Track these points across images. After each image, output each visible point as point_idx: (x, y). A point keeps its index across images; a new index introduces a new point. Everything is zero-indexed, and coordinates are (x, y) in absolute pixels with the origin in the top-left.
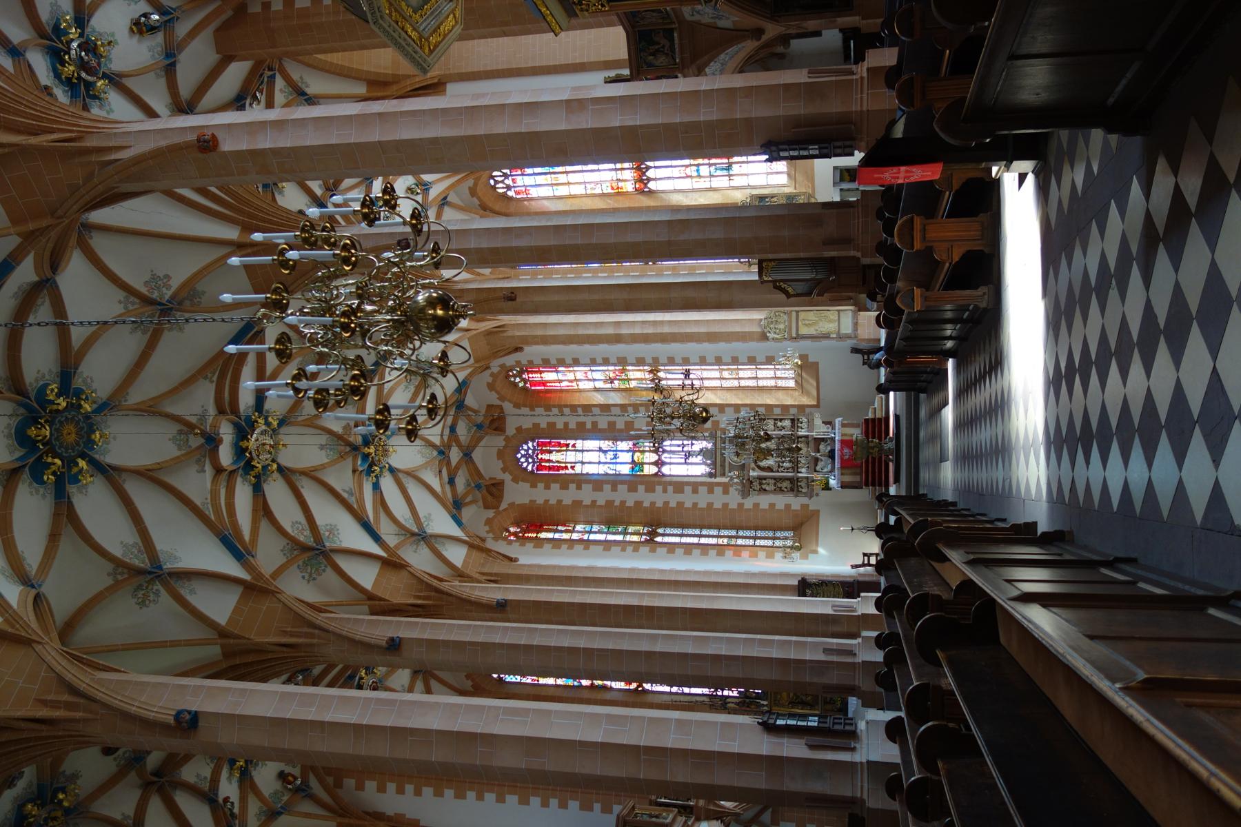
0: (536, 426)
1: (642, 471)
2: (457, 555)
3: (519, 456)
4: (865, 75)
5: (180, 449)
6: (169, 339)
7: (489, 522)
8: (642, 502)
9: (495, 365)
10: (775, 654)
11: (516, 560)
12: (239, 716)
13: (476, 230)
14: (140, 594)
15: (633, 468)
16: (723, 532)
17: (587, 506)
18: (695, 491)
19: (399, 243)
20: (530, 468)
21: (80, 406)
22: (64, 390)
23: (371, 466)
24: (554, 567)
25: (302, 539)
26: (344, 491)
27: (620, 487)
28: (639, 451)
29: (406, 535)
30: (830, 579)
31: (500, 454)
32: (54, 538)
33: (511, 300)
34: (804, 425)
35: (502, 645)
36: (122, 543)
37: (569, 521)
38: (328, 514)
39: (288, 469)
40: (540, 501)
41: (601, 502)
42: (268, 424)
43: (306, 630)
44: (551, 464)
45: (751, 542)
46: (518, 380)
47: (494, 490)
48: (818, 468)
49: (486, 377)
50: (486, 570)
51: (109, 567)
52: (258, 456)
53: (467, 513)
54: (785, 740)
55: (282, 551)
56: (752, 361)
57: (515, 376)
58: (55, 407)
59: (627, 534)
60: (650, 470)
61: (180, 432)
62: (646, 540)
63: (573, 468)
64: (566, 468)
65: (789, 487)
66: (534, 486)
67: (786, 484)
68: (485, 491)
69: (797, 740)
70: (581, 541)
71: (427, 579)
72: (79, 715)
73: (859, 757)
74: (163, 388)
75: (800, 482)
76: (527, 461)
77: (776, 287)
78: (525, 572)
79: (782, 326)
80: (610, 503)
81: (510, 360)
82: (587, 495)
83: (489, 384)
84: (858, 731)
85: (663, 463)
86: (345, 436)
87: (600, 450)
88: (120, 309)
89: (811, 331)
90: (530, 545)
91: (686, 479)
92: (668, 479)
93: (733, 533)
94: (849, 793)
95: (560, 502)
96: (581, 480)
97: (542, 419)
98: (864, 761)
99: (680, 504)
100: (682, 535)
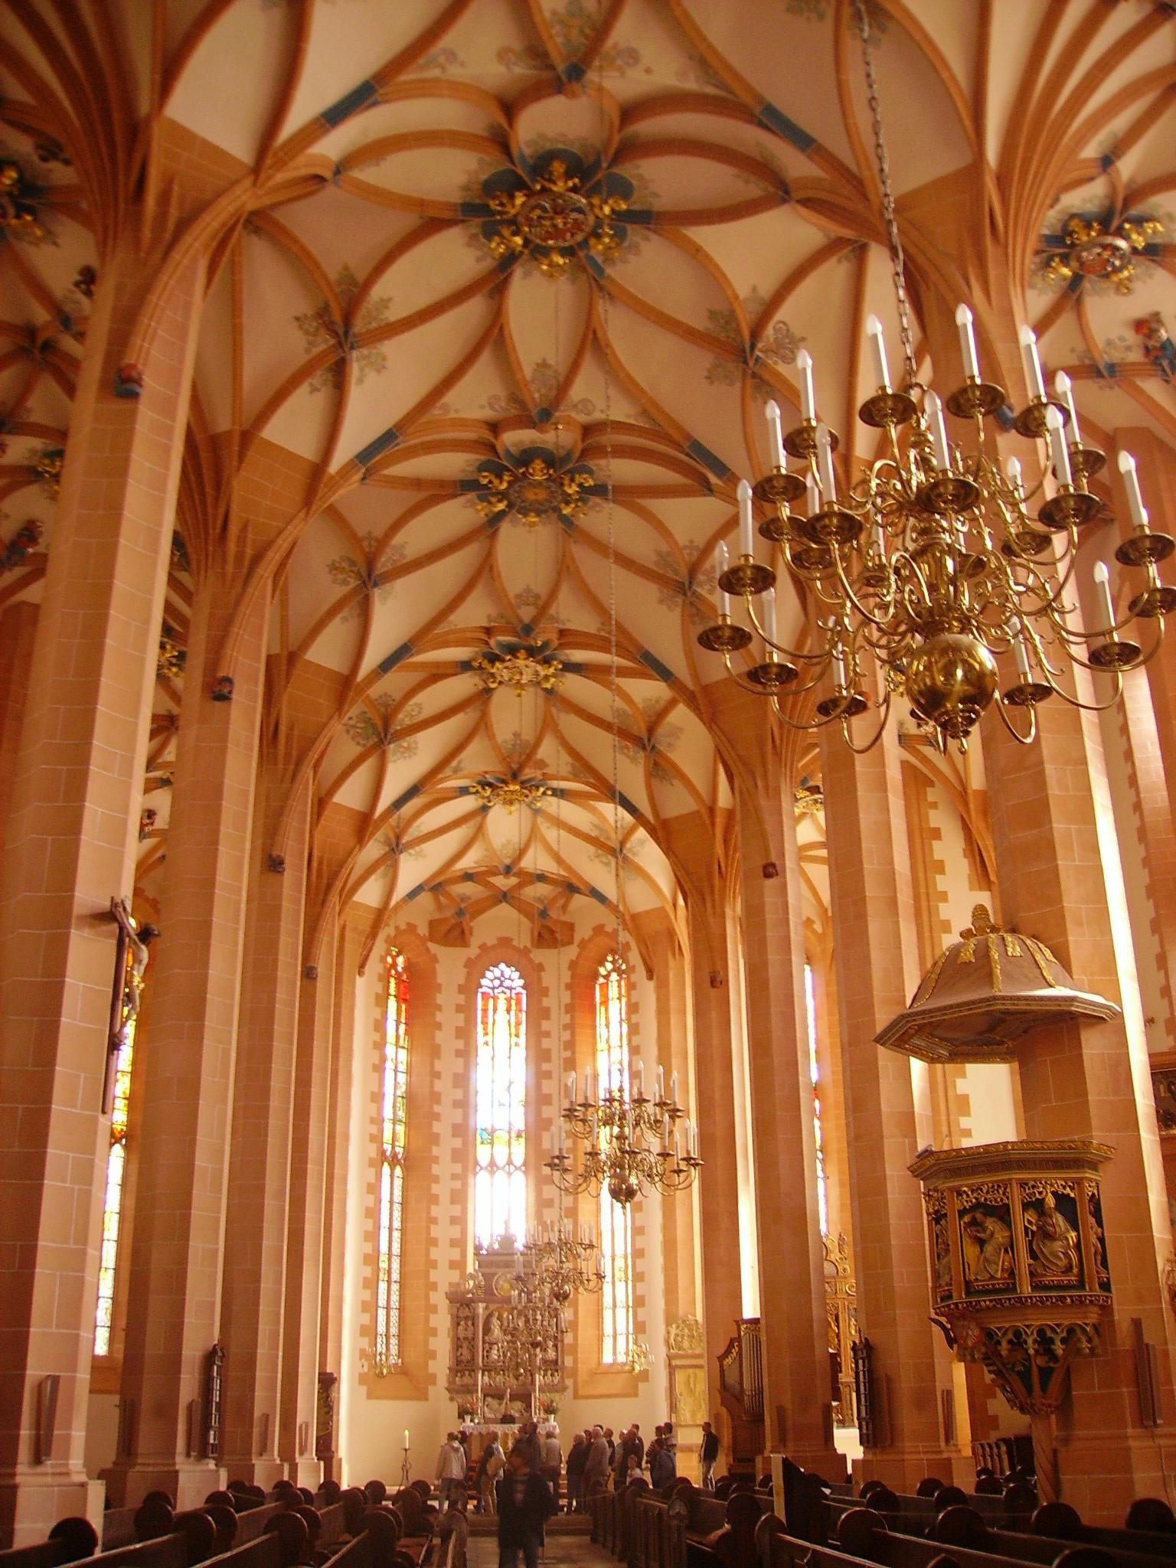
0: (545, 992)
1: (482, 1143)
2: (369, 894)
3: (502, 966)
4: (945, 1455)
5: (518, 596)
6: (652, 590)
7: (412, 928)
8: (437, 1144)
9: (624, 937)
10: (262, 1351)
11: (361, 973)
12: (224, 750)
13: (790, 961)
14: (345, 565)
15: (485, 1130)
16: (396, 1265)
17: (432, 1065)
18: (454, 1220)
19: (773, 865)
20: (484, 982)
21: (568, 503)
22: (586, 492)
23: (490, 785)
24: (351, 1028)
25: (401, 716)
26: (460, 762)
27: (460, 1111)
28: (510, 1138)
29: (398, 827)
30: (335, 1417)
31: (505, 942)
32: (417, 483)
33: (712, 980)
34: (548, 1379)
35: (272, 1000)
36: (406, 543)
37: (412, 1041)
38: (428, 746)
39: (489, 699)
40: (440, 999)
41: (438, 1086)
42: (547, 678)
43: (295, 752)
44: (490, 1012)
45: (382, 1302)
46: (609, 966)
47: (457, 932)
48: (489, 1399)
49: (611, 923)
50: (348, 934)
51: (379, 533)
52: (506, 668)
53: (425, 898)
54: (197, 1375)
55: (385, 694)
56: (639, 1302)
57: (613, 962)
58: (566, 482)
59: (394, 1124)
60: (483, 1154)
61: (537, 597)
62: (384, 1152)
63: (486, 1043)
64: (486, 1034)
65: (463, 1358)
66: (462, 989)
67: (466, 1354)
68: (453, 921)
69: (196, 1391)
70: (383, 1059)
71: (345, 871)
72: (230, 568)
73: (180, 1458)
74: (590, 581)
76: (496, 978)
77: (732, 1341)
78: (345, 979)
79: (686, 1344)
80: (436, 1098)
81: (634, 957)
82: (447, 1065)
83: (602, 926)
84: (207, 1460)
85: (492, 1173)
86: (531, 763)
87: (511, 1083)
88: (682, 539)
89: (679, 1387)
90: (379, 988)
91: (470, 1206)
92: (471, 1181)
93: (395, 1276)
94: (140, 1450)
95: (439, 1026)
96: (467, 1053)
97: (557, 998)
98: (177, 1467)
99: (434, 1199)
100: (391, 1202)
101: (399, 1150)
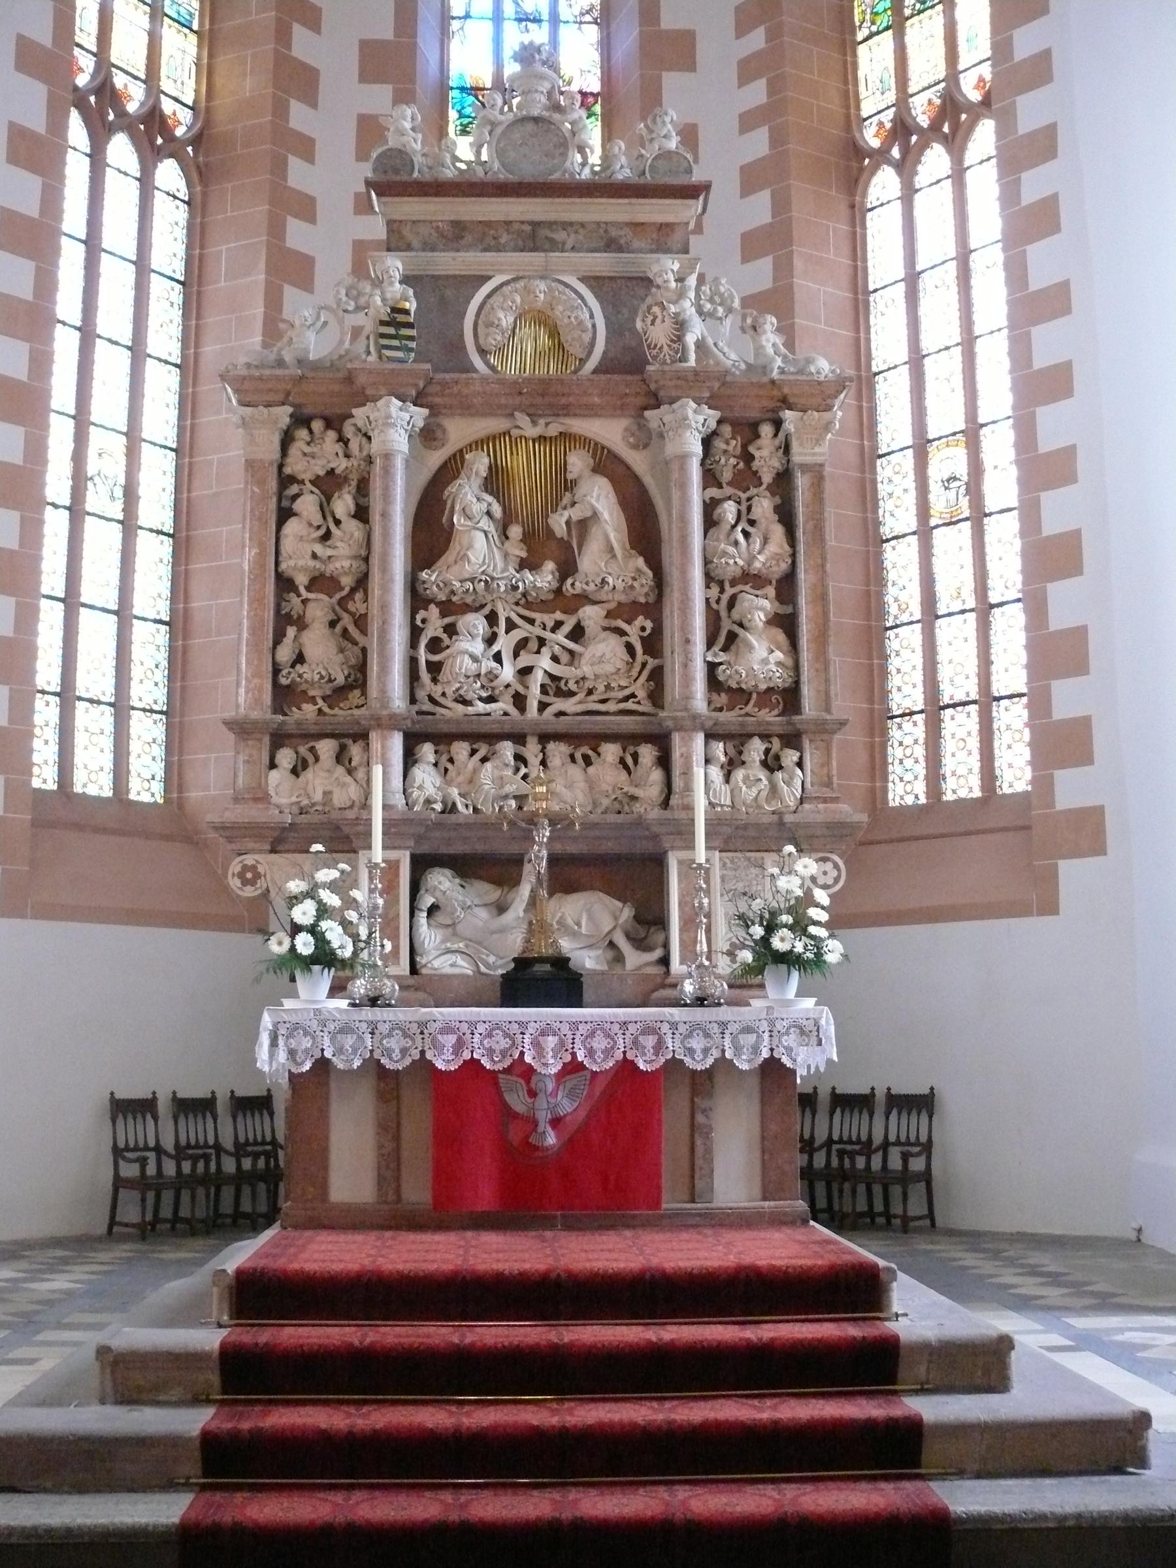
15: (475, 90)
48: (441, 881)
75: (341, 757)
101: (182, 121)
